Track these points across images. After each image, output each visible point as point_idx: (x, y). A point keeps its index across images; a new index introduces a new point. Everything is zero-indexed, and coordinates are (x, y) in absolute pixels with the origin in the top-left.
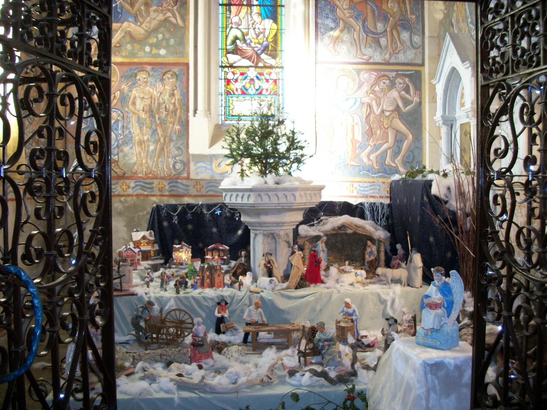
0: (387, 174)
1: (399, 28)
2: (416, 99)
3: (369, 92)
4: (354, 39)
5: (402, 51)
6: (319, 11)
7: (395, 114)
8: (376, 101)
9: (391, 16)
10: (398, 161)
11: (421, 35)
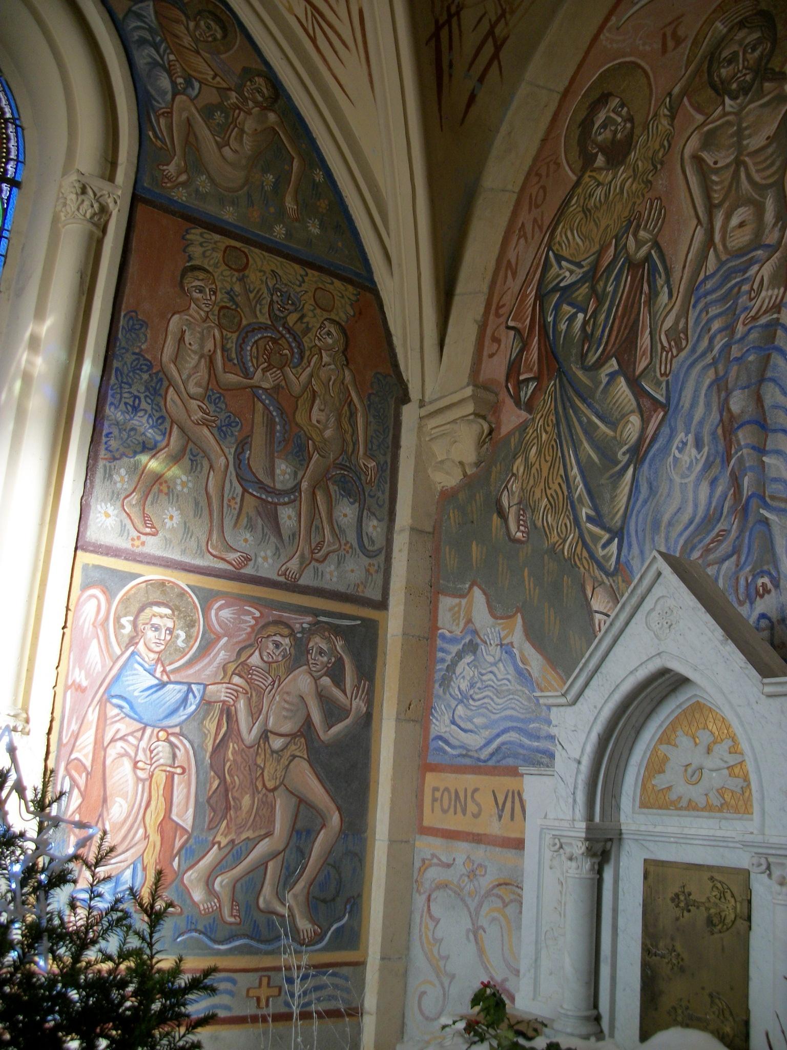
0: (260, 941)
1: (333, 488)
2: (358, 705)
3: (232, 667)
4: (207, 493)
5: (334, 557)
6: (113, 380)
7: (299, 748)
8: (249, 699)
9: (316, 448)
10: (295, 896)
11: (386, 518)
